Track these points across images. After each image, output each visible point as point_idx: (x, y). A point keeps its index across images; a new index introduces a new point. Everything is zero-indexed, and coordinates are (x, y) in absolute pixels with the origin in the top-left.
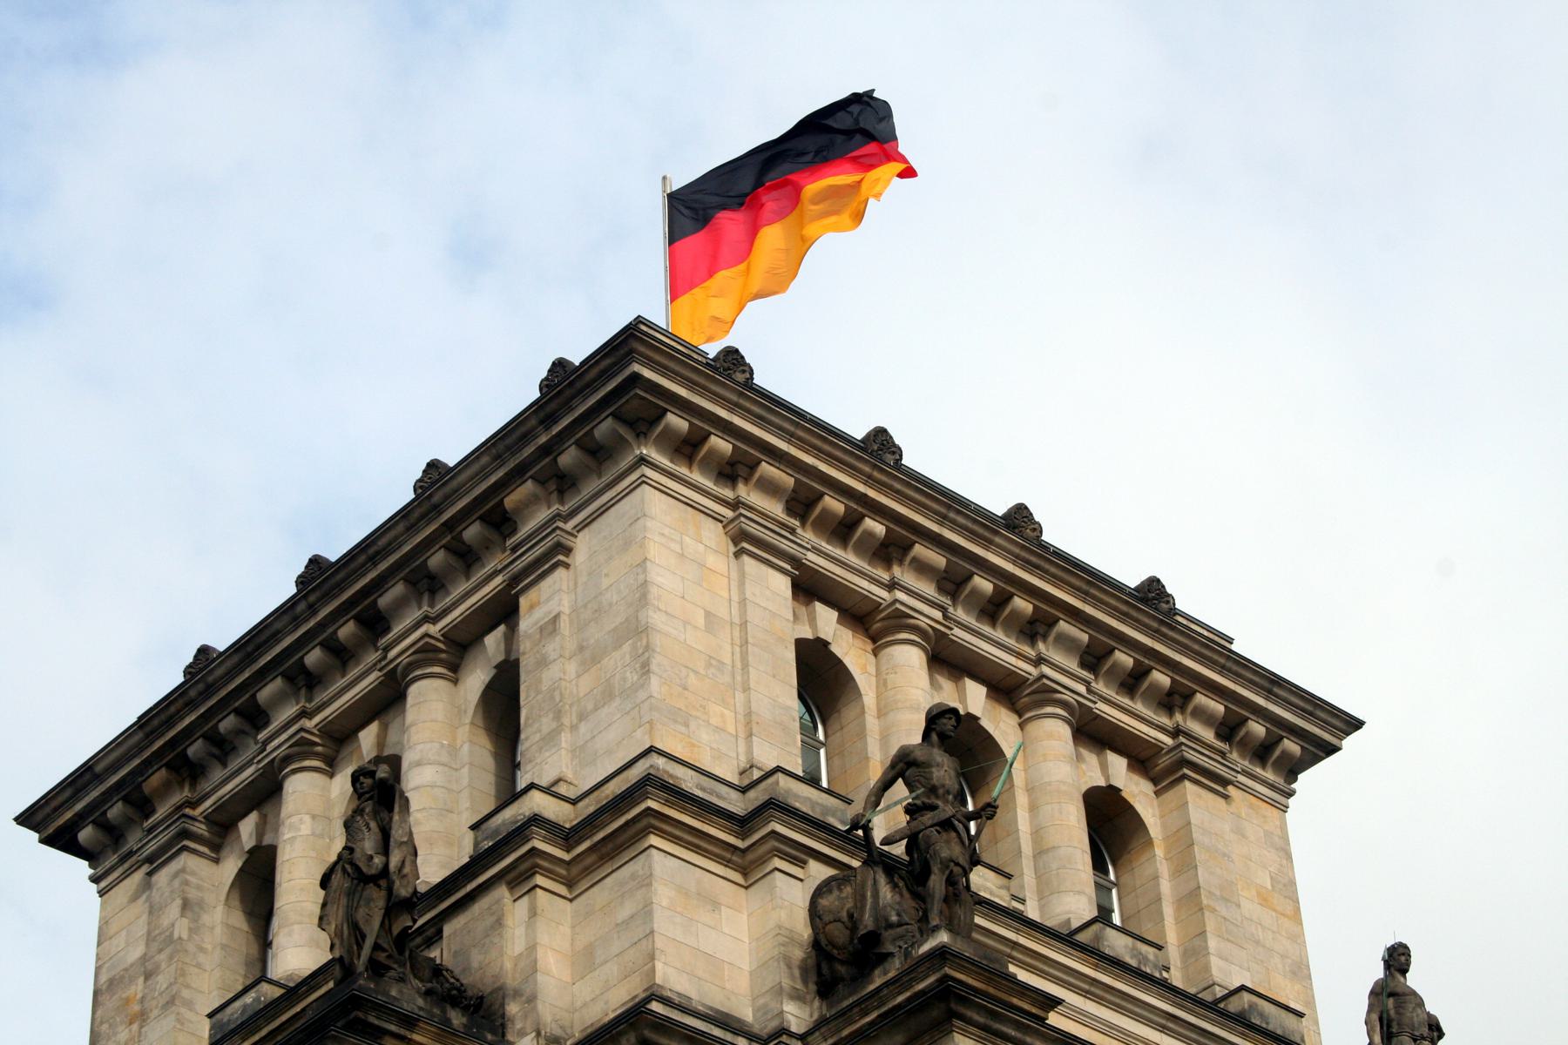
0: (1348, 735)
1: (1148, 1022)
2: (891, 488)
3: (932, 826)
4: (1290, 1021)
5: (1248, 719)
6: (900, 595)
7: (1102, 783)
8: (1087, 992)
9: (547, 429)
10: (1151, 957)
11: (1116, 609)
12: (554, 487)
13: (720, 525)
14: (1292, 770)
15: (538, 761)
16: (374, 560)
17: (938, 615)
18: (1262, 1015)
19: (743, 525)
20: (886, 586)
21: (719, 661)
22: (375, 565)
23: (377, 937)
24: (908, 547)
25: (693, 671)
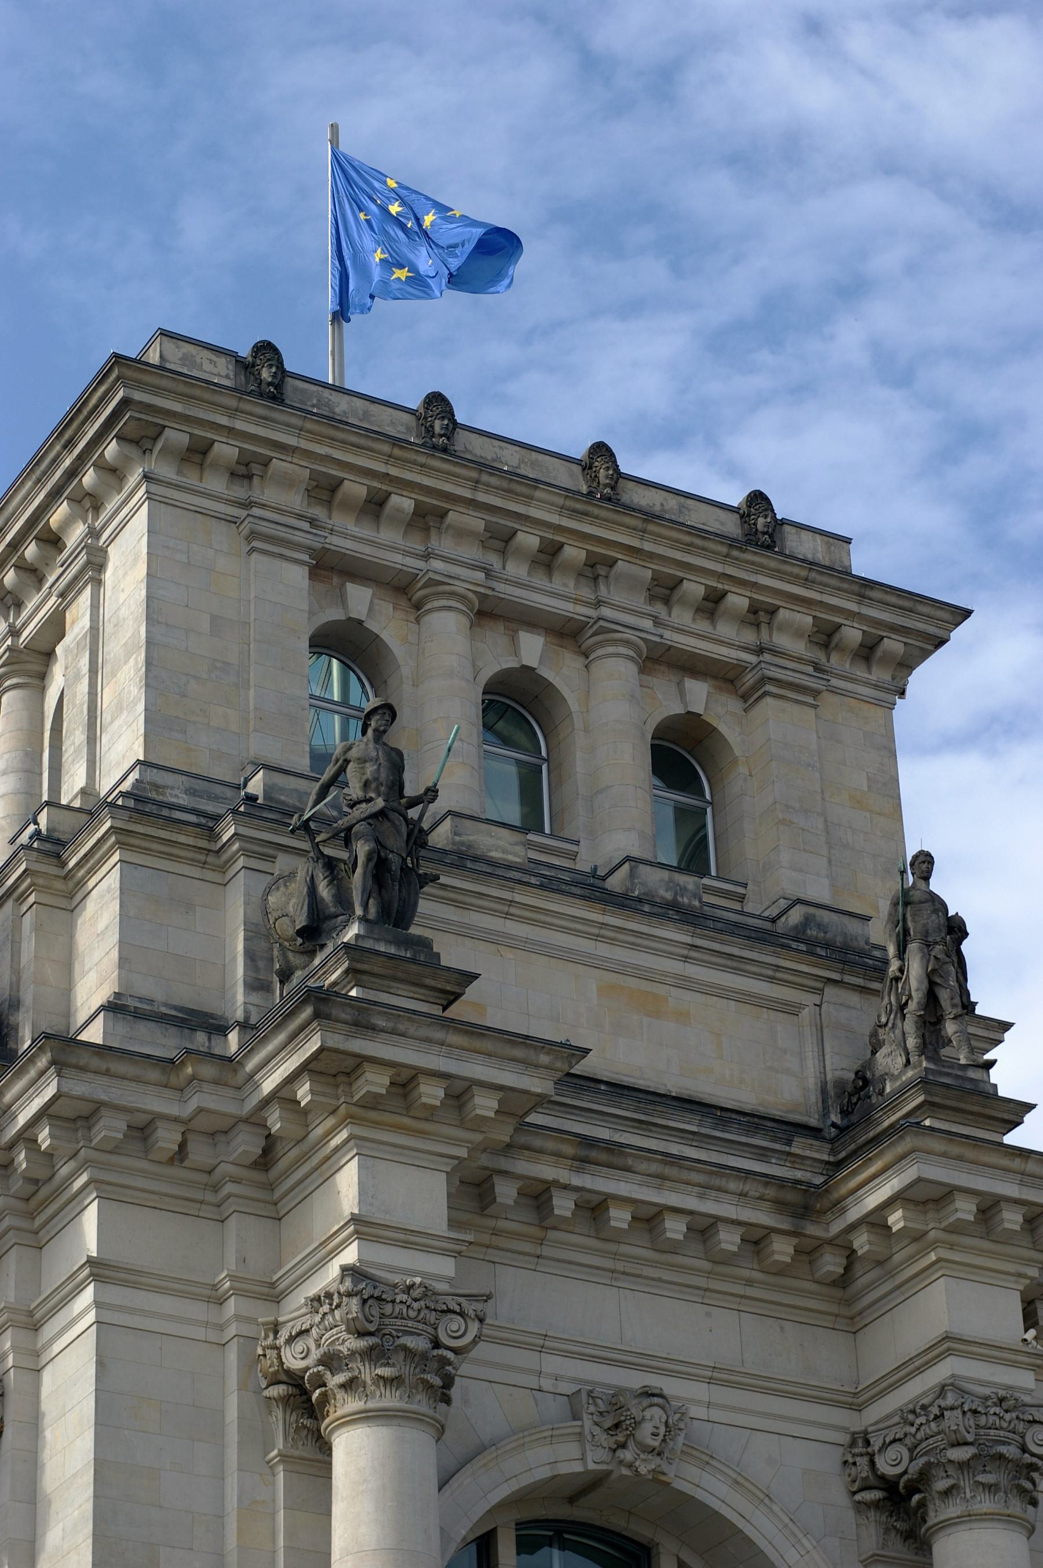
1: (670, 955)
2: (415, 463)
4: (853, 927)
5: (840, 626)
6: (437, 565)
7: (678, 709)
10: (691, 887)
11: (677, 541)
12: (89, 505)
14: (907, 665)
15: (72, 772)
17: (480, 576)
18: (820, 926)
21: (224, 662)
24: (443, 515)
25: (195, 677)
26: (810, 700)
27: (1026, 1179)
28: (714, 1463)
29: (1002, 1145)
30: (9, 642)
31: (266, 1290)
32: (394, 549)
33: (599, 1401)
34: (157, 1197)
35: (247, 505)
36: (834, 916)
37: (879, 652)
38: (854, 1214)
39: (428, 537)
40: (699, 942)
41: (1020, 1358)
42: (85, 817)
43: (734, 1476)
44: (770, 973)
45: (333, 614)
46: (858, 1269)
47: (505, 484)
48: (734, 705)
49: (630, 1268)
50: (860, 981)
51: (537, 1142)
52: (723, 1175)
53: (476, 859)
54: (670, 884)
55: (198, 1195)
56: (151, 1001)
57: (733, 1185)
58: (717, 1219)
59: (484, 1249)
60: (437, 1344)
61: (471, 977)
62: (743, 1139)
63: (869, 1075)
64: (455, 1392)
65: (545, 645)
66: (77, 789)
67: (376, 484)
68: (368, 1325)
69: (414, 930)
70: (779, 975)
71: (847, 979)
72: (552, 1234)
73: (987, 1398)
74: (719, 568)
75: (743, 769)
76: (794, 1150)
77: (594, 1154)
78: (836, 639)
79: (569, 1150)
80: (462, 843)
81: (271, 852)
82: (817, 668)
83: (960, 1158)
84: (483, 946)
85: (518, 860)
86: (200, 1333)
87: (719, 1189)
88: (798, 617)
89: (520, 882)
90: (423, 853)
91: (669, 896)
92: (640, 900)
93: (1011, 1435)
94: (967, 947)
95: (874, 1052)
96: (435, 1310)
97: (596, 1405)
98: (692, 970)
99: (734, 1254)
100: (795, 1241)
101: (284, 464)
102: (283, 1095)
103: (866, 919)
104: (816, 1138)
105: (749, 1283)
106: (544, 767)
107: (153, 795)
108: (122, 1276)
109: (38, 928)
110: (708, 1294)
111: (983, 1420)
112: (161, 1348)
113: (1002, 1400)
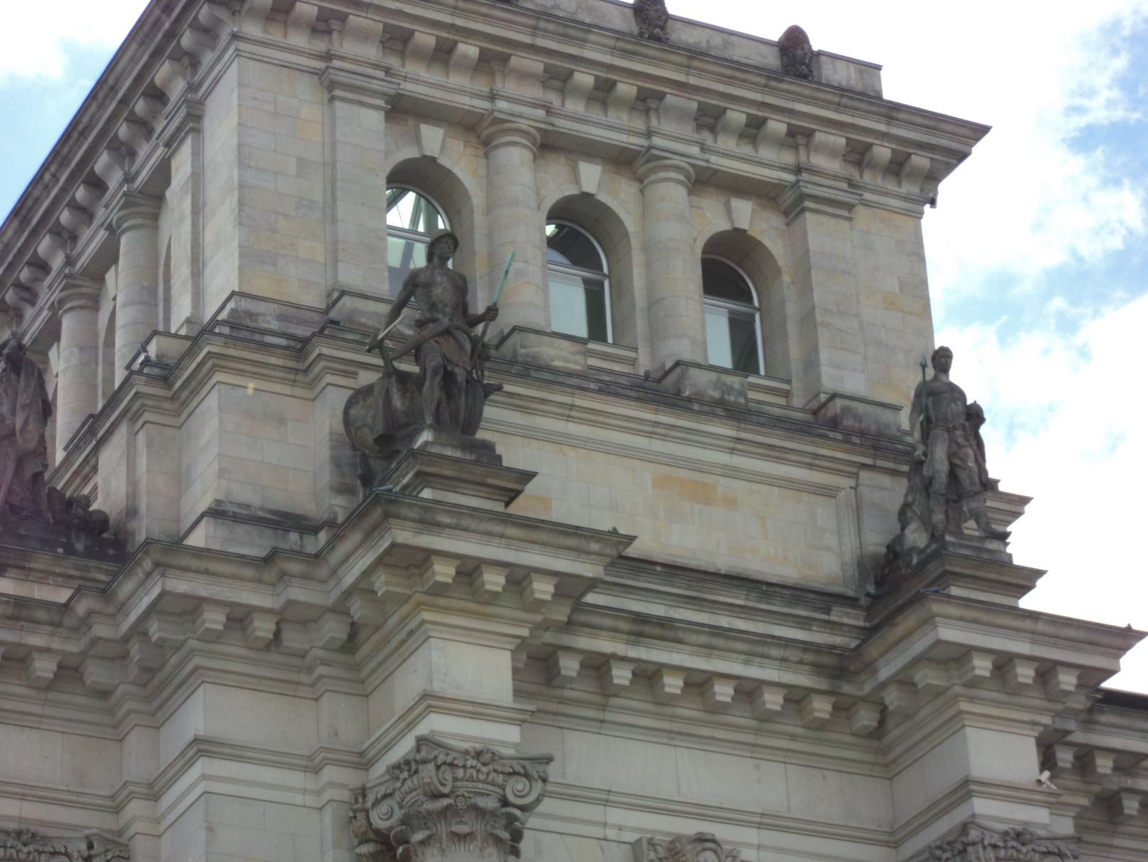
0: (977, 140)
2: (478, 13)
3: (431, 338)
4: (887, 416)
6: (502, 104)
7: (724, 226)
8: (651, 433)
9: (169, 15)
10: (737, 386)
13: (316, 77)
14: (933, 177)
16: (83, 135)
17: (541, 113)
18: (857, 417)
19: (331, 76)
20: (488, 97)
22: (86, 138)
23: (12, 484)
24: (505, 59)
26: (845, 213)
27: (1036, 637)
29: (1018, 609)
30: (125, 188)
31: (356, 759)
32: (462, 92)
33: (659, 848)
34: (255, 680)
35: (328, 57)
36: (868, 408)
37: (907, 168)
38: (884, 673)
39: (494, 80)
40: (744, 435)
41: (1035, 797)
42: (188, 343)
44: (809, 460)
45: (410, 153)
46: (890, 723)
47: (561, 30)
48: (776, 220)
49: (685, 729)
50: (891, 465)
51: (596, 620)
52: (765, 643)
53: (540, 368)
54: (717, 385)
55: (294, 677)
56: (248, 506)
57: (774, 652)
58: (762, 683)
59: (552, 717)
60: (505, 803)
61: (528, 476)
62: (786, 610)
63: (898, 548)
64: (524, 846)
65: (603, 172)
66: (183, 318)
67: (444, 34)
68: (441, 788)
69: (481, 435)
70: (817, 462)
71: (879, 463)
72: (613, 701)
73: (1006, 833)
74: (758, 97)
76: (833, 618)
77: (648, 629)
78: (867, 158)
80: (527, 355)
81: (352, 369)
82: (851, 184)
84: (547, 446)
85: (578, 368)
86: (298, 799)
88: (832, 139)
89: (580, 388)
90: (487, 364)
92: (689, 400)
94: (984, 431)
95: (903, 529)
96: (502, 773)
97: (656, 851)
99: (778, 713)
100: (833, 699)
101: (360, 20)
102: (362, 588)
103: (896, 408)
104: (853, 607)
105: (793, 737)
106: (606, 283)
107: (248, 322)
108: (228, 751)
109: (150, 443)
110: (757, 749)
111: (1002, 853)
112: (264, 814)
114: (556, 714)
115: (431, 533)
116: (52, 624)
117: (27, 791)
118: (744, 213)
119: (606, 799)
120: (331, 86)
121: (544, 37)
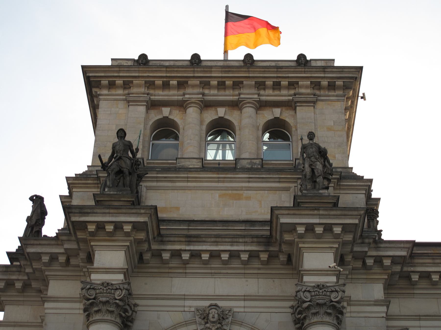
2: (174, 71)
6: (187, 96)
8: (218, 181)
17: (201, 96)
24: (187, 82)
26: (312, 104)
27: (321, 216)
28: (243, 324)
33: (200, 311)
37: (336, 86)
43: (251, 327)
44: (278, 180)
45: (160, 117)
51: (172, 239)
52: (236, 238)
54: (250, 163)
57: (241, 240)
59: (167, 274)
62: (261, 228)
70: (281, 180)
73: (314, 286)
74: (275, 75)
75: (293, 129)
79: (183, 239)
83: (294, 214)
84: (180, 191)
87: (237, 242)
88: (305, 82)
91: (250, 166)
93: (324, 297)
96: (112, 289)
97: (199, 312)
98: (251, 185)
100: (268, 253)
101: (137, 81)
105: (259, 269)
108: (52, 299)
110: (245, 275)
111: (313, 294)
112: (65, 318)
113: (318, 286)
114: (169, 273)
115: (85, 216)
116: (18, 272)
117: (15, 324)
118: (277, 112)
119: (184, 298)
120: (129, 102)
121: (198, 73)
